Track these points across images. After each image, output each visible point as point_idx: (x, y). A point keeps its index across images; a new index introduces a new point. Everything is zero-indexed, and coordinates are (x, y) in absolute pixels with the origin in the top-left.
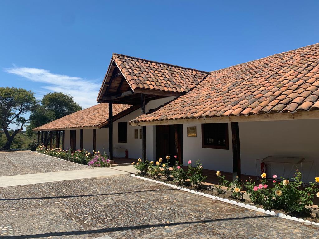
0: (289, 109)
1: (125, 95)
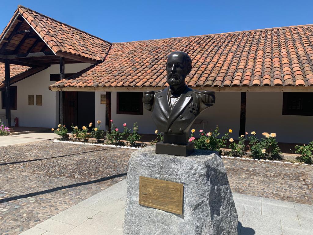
0: (218, 85)
1: (34, 56)
